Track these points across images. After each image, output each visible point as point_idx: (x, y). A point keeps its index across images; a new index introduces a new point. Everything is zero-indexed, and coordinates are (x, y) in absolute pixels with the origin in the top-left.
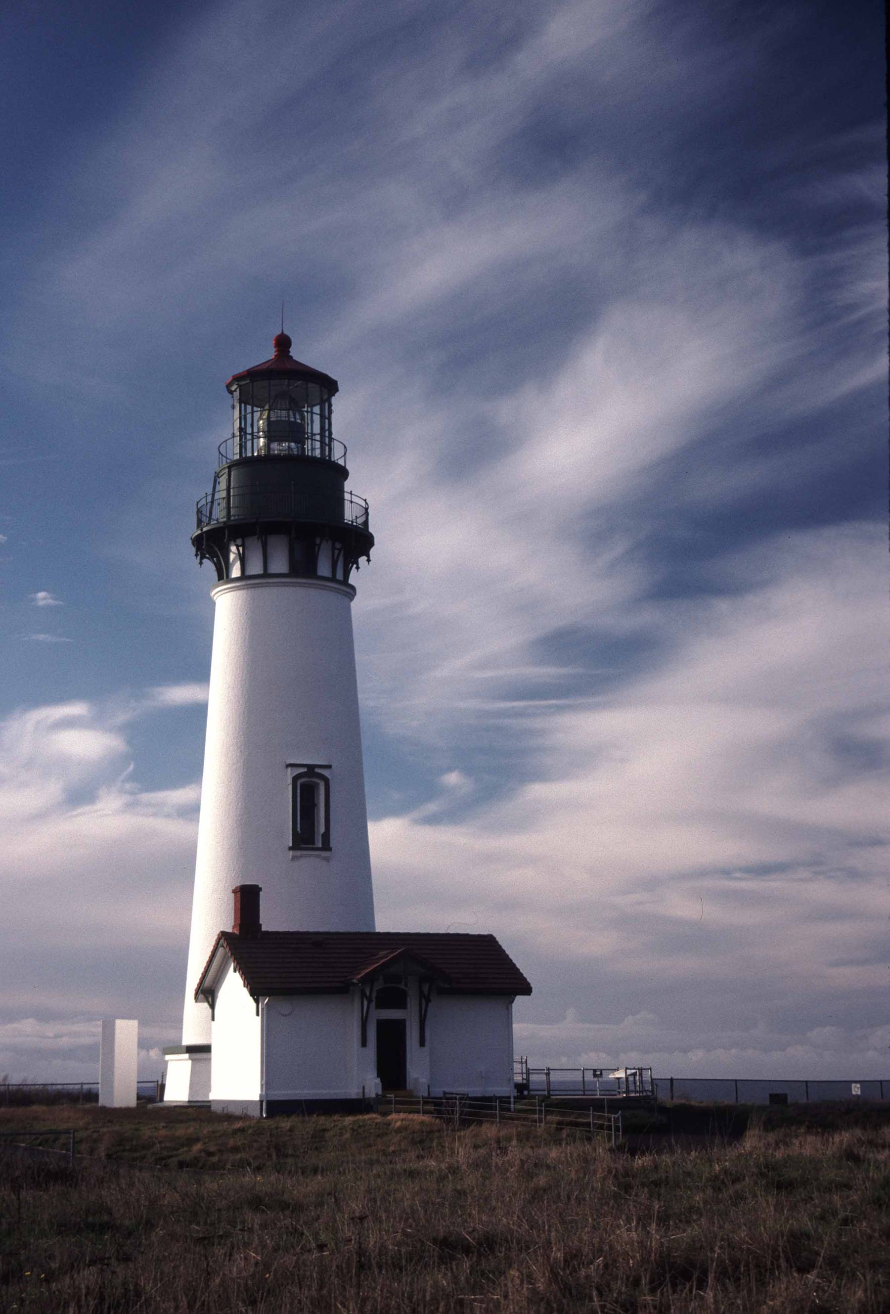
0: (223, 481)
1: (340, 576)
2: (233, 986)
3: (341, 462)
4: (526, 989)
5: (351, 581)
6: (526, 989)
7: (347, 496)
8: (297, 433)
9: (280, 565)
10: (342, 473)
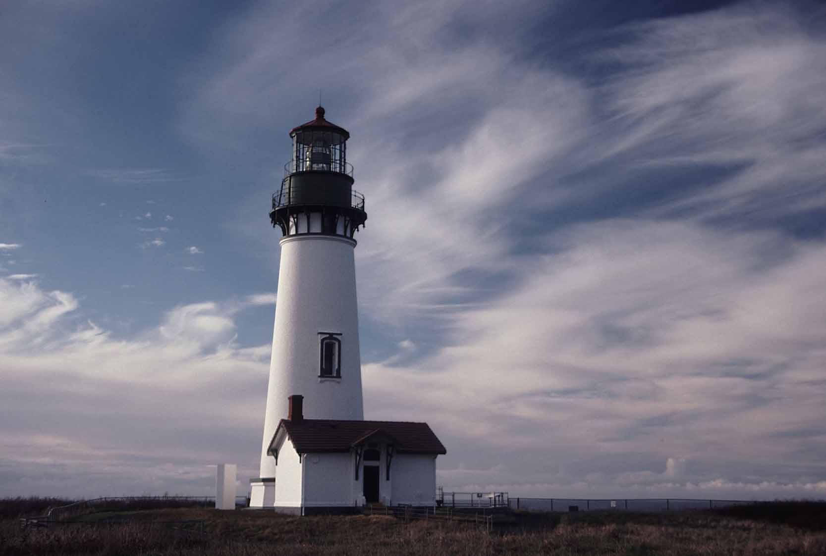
0: (287, 183)
1: (348, 235)
2: (288, 448)
3: (350, 175)
4: (444, 452)
6: (444, 452)
7: (353, 193)
8: (328, 160)
9: (316, 228)
10: (351, 180)
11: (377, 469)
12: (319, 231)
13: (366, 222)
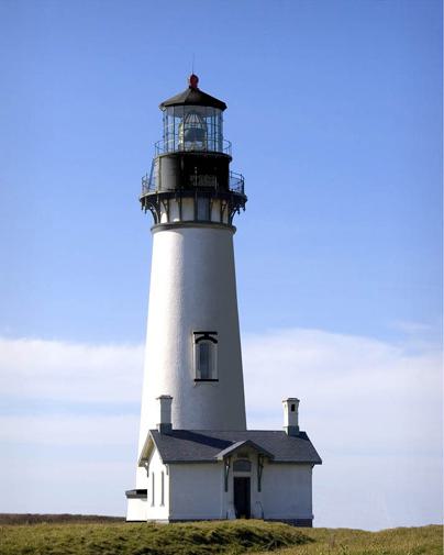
0: (157, 164)
1: (225, 221)
2: (156, 457)
4: (320, 462)
5: (233, 224)
6: (320, 462)
9: (189, 215)
10: (228, 159)
11: (247, 481)
12: (192, 219)
13: (246, 204)
